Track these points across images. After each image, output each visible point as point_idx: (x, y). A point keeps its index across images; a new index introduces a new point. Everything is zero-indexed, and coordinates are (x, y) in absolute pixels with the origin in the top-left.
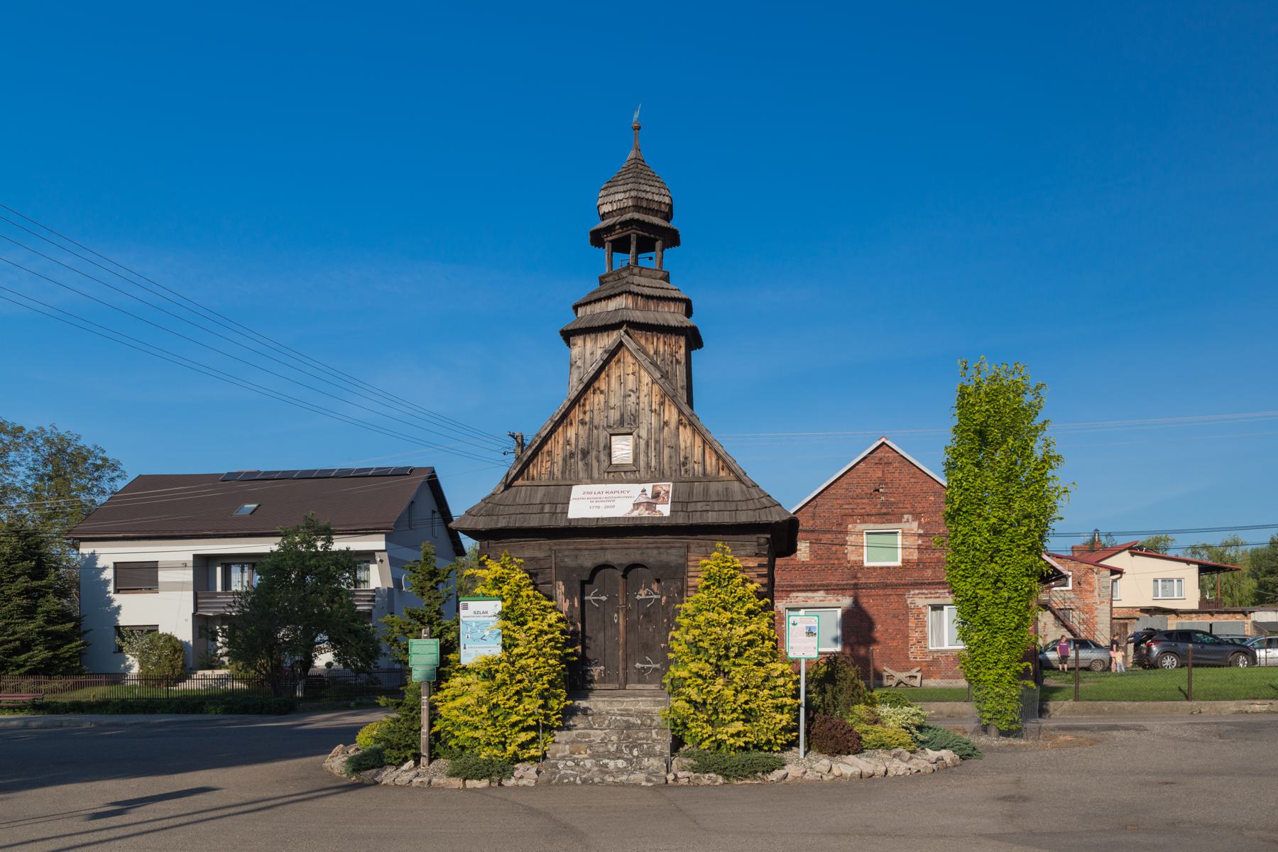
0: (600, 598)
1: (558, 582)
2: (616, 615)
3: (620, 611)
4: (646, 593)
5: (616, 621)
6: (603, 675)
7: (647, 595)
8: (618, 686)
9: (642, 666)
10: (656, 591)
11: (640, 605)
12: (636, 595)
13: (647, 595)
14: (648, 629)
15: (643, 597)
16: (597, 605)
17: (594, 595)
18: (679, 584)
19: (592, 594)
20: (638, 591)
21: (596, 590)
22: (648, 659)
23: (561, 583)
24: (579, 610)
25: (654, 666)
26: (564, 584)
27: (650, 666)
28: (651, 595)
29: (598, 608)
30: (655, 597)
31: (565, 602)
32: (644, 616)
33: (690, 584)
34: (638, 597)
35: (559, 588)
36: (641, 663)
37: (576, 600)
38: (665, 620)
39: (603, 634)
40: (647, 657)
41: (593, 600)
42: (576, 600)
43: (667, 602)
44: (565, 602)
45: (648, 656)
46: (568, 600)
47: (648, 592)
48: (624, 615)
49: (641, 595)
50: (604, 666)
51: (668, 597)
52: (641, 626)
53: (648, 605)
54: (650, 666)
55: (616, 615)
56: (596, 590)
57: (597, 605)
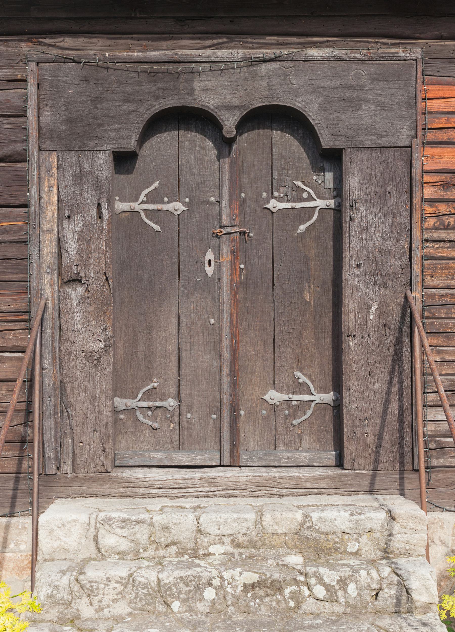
0: (165, 207)
2: (210, 255)
5: (210, 271)
9: (285, 397)
17: (151, 199)
19: (142, 197)
21: (156, 184)
27: (307, 398)
36: (281, 391)
39: (174, 309)
40: (298, 374)
41: (144, 210)
48: (233, 252)
54: (307, 398)
55: (210, 255)
56: (156, 184)
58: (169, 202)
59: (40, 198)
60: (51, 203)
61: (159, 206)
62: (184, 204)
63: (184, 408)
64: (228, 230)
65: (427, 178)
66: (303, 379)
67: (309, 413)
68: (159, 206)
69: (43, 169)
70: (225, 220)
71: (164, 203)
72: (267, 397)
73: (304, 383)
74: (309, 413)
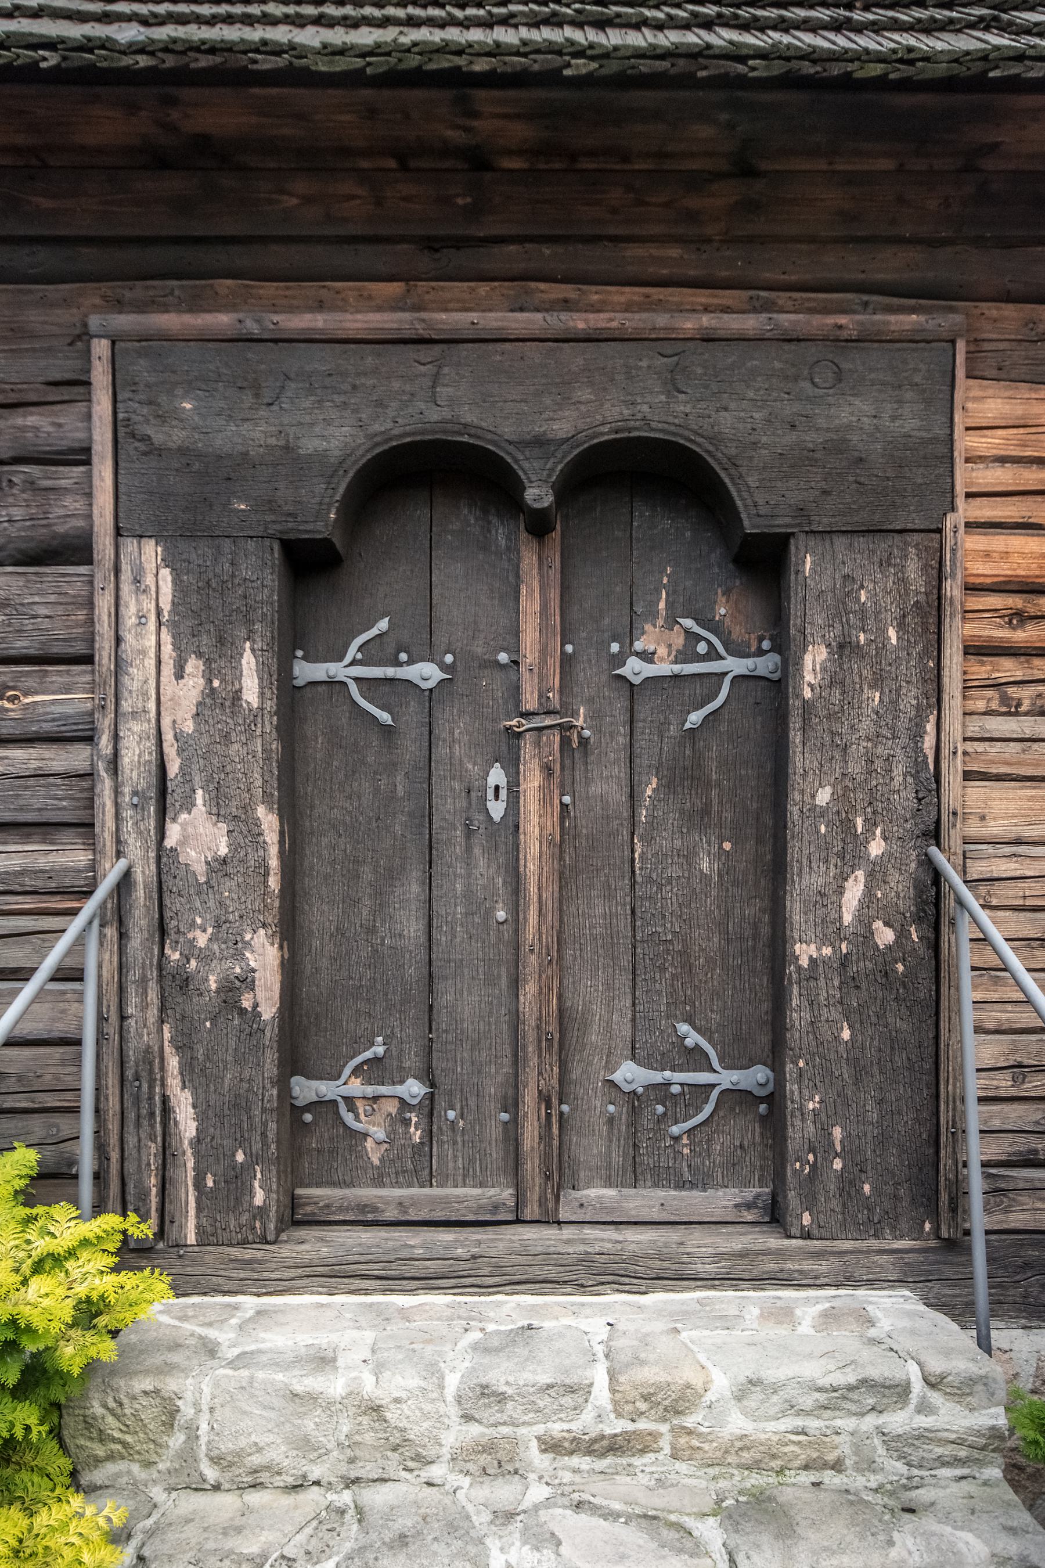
1: (130, 545)
3: (527, 748)
4: (679, 641)
6: (417, 1136)
7: (686, 655)
8: (506, 1194)
10: (738, 633)
11: (643, 711)
12: (619, 660)
13: (686, 655)
14: (689, 857)
15: (664, 668)
16: (385, 717)
17: (370, 655)
18: (913, 569)
19: (352, 652)
20: (631, 635)
21: (383, 625)
22: (693, 1038)
23: (151, 552)
24: (269, 725)
25: (727, 1078)
26: (167, 562)
28: (712, 655)
29: (387, 731)
30: (735, 666)
31: (179, 675)
32: (669, 786)
33: (982, 570)
34: (634, 669)
35: (137, 581)
36: (647, 1063)
37: (248, 662)
38: (824, 796)
41: (356, 679)
42: (248, 662)
43: (835, 680)
44: (179, 675)
45: (690, 1020)
46: (194, 666)
47: (692, 637)
49: (648, 657)
50: (428, 1076)
51: (844, 648)
52: (648, 840)
53: (695, 718)
56: (383, 625)
57: (385, 717)
58: (410, 662)
59: (118, 640)
60: (143, 652)
61: (390, 672)
62: (444, 667)
63: (441, 1103)
64: (537, 722)
65: (976, 602)
66: (693, 1038)
67: (708, 1109)
68: (390, 672)
69: (126, 576)
70: (530, 701)
71: (400, 664)
72: (617, 1077)
73: (697, 1047)
74: (708, 1109)
